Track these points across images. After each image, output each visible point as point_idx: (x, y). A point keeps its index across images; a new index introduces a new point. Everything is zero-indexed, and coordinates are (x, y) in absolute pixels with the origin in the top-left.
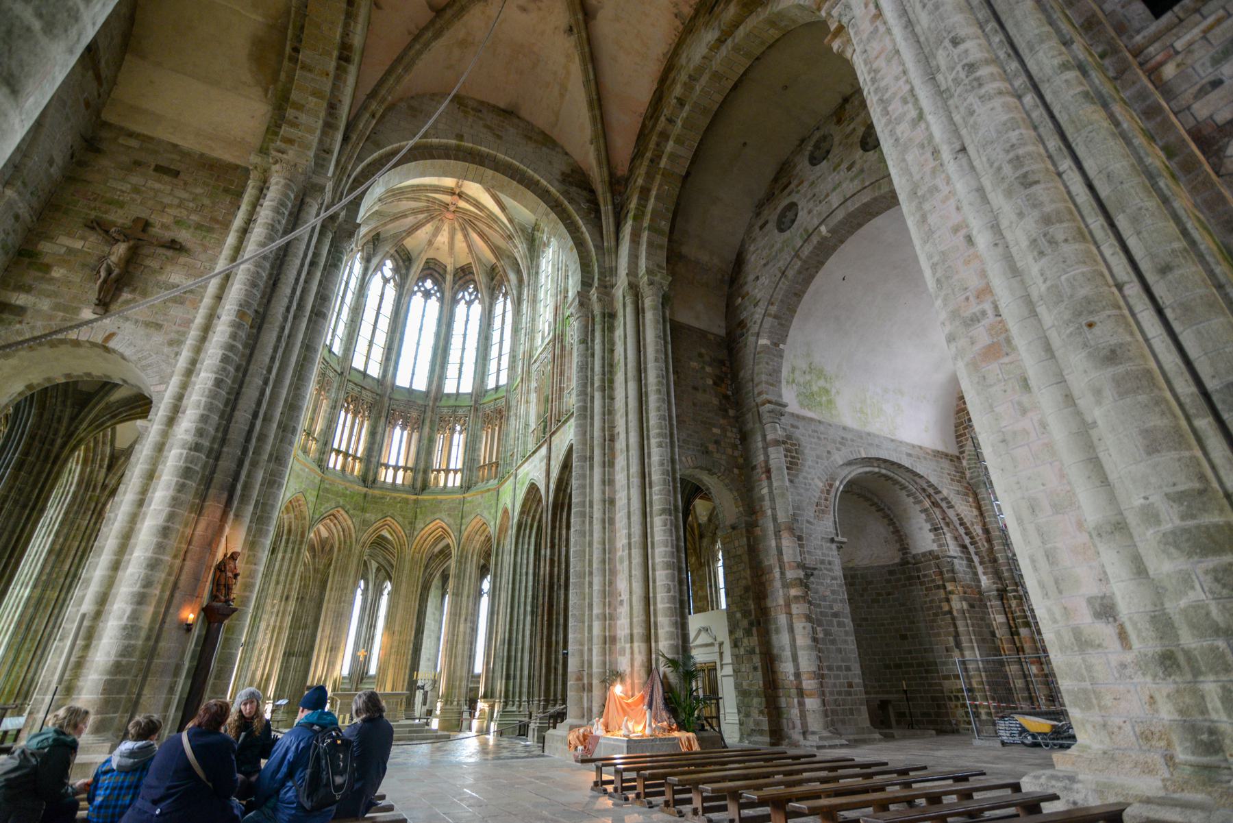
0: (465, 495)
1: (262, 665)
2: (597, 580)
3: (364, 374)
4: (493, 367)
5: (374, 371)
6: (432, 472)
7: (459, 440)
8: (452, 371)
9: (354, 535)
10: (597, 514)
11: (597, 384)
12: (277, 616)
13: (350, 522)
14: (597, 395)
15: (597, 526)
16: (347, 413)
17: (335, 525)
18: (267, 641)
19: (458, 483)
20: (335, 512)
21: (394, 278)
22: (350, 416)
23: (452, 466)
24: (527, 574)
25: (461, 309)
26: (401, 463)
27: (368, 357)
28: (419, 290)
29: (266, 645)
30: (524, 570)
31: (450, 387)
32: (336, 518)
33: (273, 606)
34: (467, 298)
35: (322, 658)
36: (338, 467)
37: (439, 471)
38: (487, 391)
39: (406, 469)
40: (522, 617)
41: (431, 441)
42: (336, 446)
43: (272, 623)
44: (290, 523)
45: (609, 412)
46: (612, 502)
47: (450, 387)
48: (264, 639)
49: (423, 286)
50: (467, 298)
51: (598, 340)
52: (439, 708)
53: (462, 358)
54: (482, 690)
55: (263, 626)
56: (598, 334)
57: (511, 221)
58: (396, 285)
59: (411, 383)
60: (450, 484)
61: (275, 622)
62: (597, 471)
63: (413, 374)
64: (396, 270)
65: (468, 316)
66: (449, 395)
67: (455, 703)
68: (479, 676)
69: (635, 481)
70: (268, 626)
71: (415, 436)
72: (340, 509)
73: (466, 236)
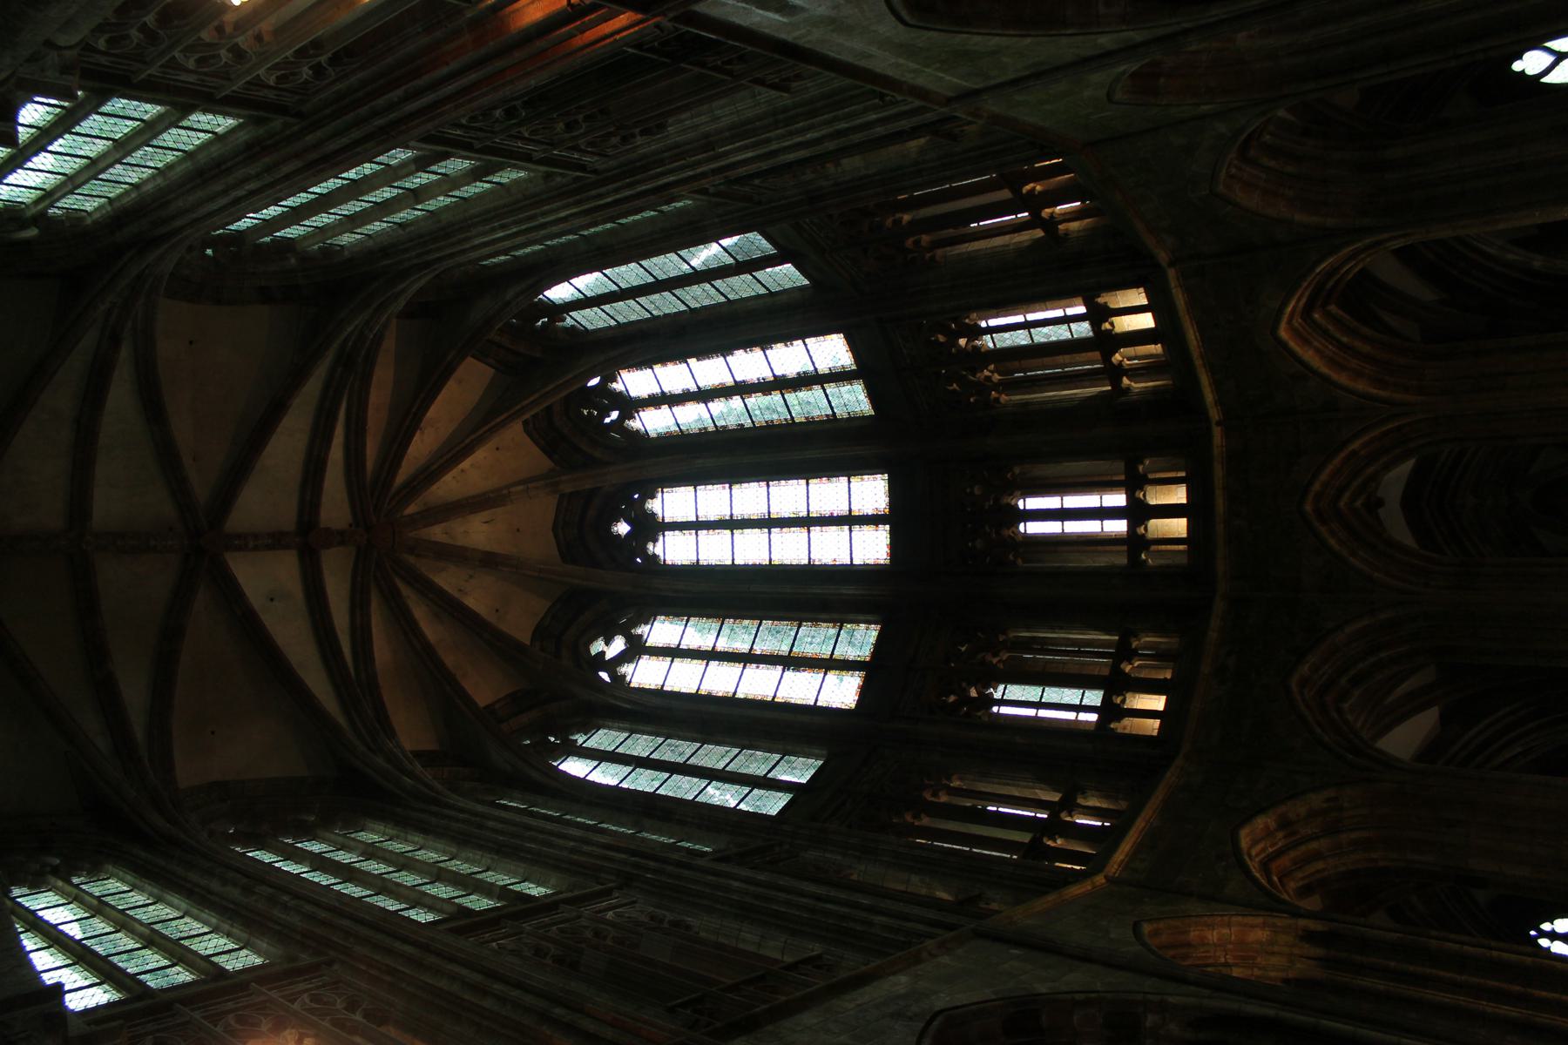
0: (1163, 257)
3: (873, 670)
4: (741, 287)
5: (860, 640)
6: (1128, 389)
8: (809, 404)
19: (1138, 298)
23: (1083, 329)
25: (654, 422)
26: (1118, 499)
31: (854, 399)
34: (615, 415)
36: (1157, 703)
37: (1115, 372)
39: (1133, 484)
41: (1028, 418)
47: (854, 399)
53: (764, 387)
57: (299, 376)
58: (648, 619)
60: (1146, 321)
73: (430, 473)
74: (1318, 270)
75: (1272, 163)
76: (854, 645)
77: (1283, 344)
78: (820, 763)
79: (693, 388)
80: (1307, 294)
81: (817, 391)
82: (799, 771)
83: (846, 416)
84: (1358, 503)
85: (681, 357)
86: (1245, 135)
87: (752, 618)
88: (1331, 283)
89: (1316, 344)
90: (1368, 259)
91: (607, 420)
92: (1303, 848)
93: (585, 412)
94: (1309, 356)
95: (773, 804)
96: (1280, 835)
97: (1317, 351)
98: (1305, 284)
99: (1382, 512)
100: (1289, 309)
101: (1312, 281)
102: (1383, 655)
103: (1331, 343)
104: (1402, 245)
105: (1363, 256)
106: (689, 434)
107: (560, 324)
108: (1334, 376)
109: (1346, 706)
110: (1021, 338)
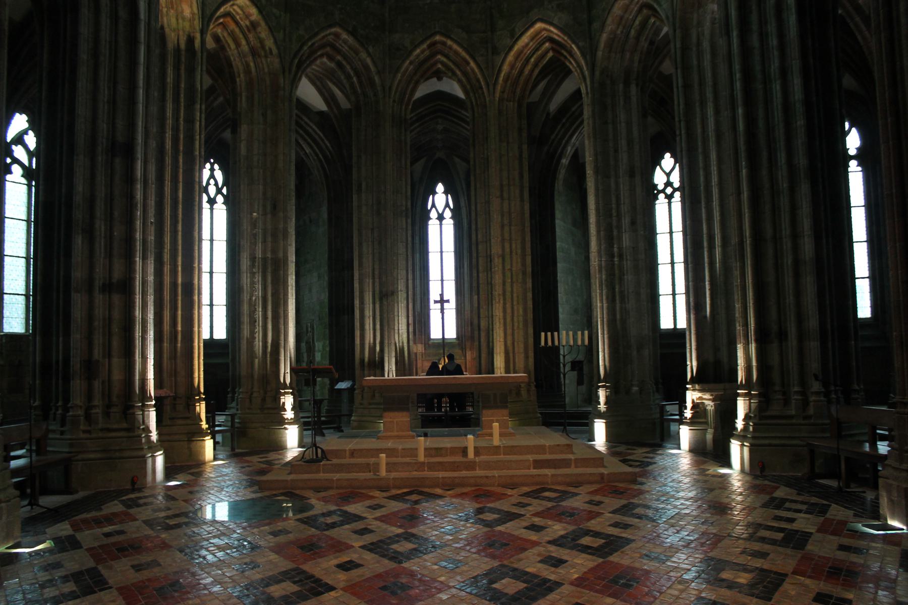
1: (259, 330)
9: (377, 79)
12: (264, 241)
13: (363, 55)
17: (339, 65)
18: (259, 287)
20: (330, 38)
24: (784, 72)
29: (260, 293)
30: (775, 66)
32: (338, 51)
33: (254, 225)
35: (368, 313)
40: (784, 185)
43: (259, 254)
44: (247, 71)
48: (253, 283)
52: (602, 399)
54: (692, 364)
55: (245, 263)
61: (264, 251)
67: (635, 389)
68: (677, 335)
70: (253, 259)
72: (337, 29)
74: (573, 46)
75: (637, 22)
77: (532, 24)
80: (560, 39)
84: (440, 66)
86: (656, 6)
88: (565, 53)
89: (531, 44)
90: (576, 73)
92: (241, 36)
94: (525, 39)
96: (248, 23)
97: (527, 45)
98: (566, 38)
99: (435, 79)
100: (552, 29)
101: (567, 43)
102: (355, 79)
103: (530, 53)
104: (582, 92)
105: (579, 71)
108: (512, 53)
109: (325, 60)
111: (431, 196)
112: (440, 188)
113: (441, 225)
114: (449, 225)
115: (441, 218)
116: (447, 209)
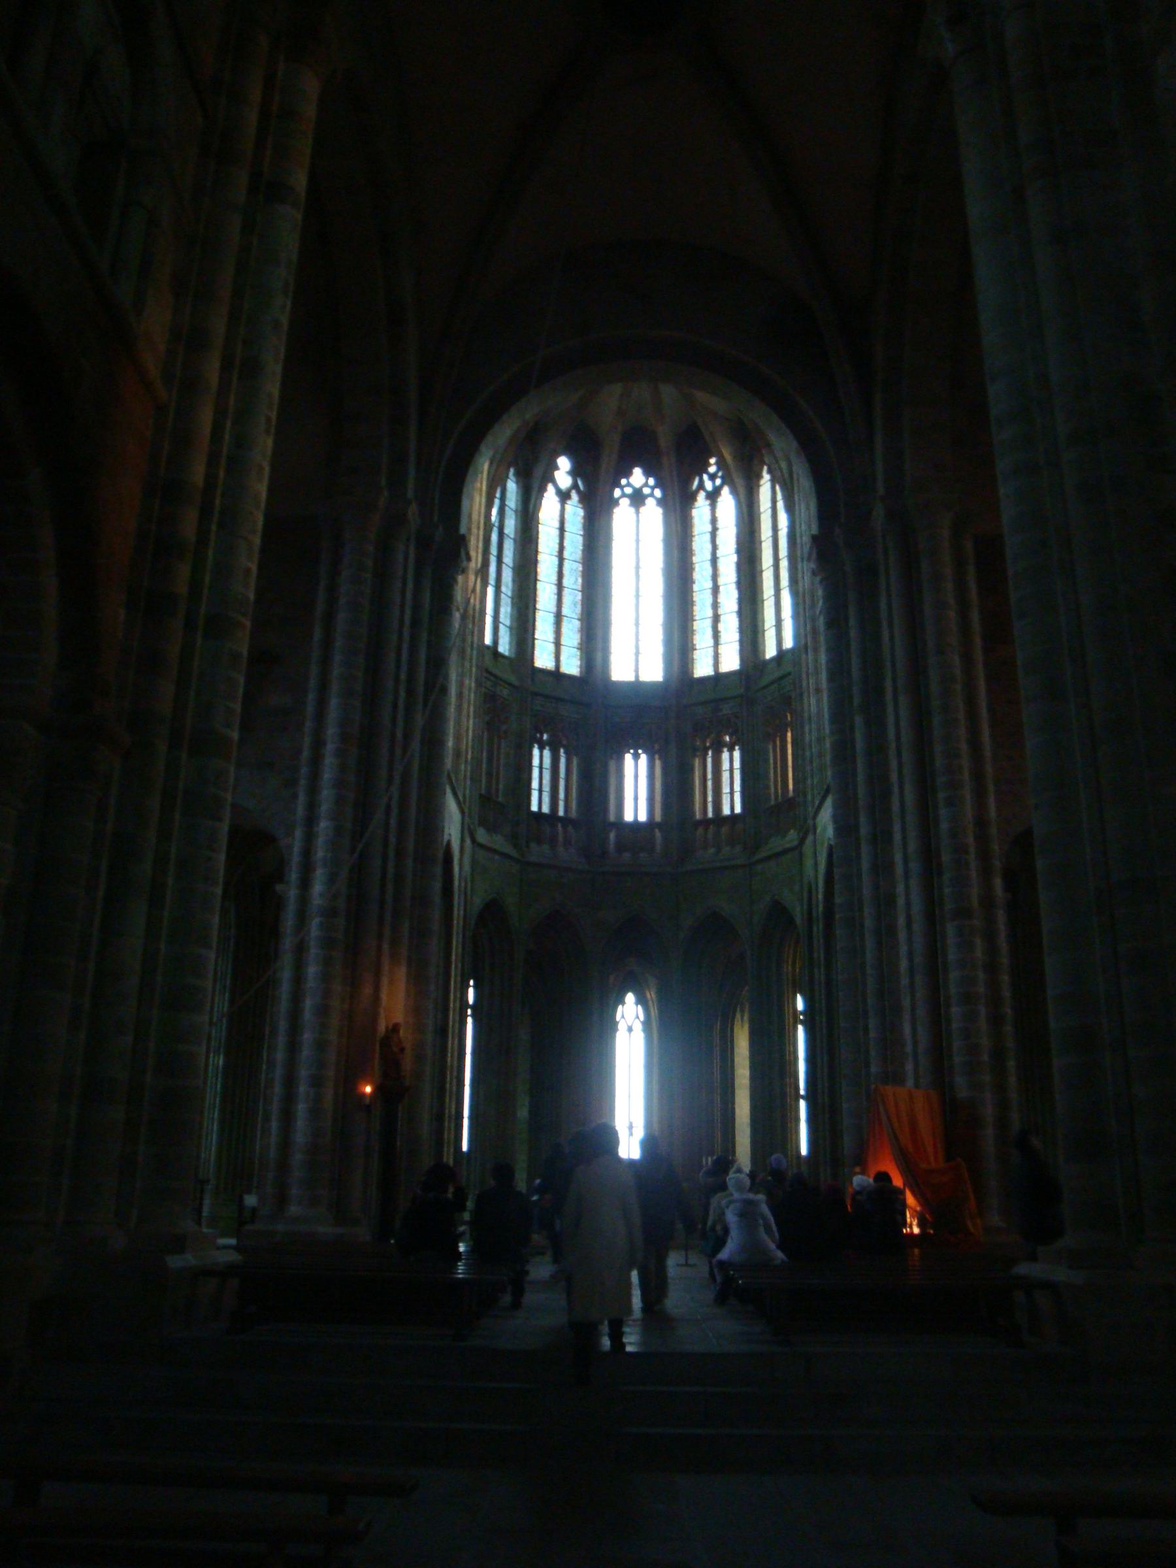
2: (872, 1023)
3: (556, 675)
5: (571, 666)
7: (732, 761)
10: (869, 923)
11: (857, 701)
14: (858, 720)
15: (870, 943)
16: (541, 749)
21: (575, 486)
22: (547, 753)
27: (558, 644)
28: (624, 495)
31: (702, 668)
38: (766, 663)
42: (534, 807)
45: (877, 747)
46: (891, 900)
49: (629, 485)
50: (709, 485)
51: (852, 622)
53: (715, 605)
56: (852, 611)
59: (637, 671)
62: (865, 850)
63: (637, 653)
64: (574, 473)
65: (714, 521)
66: (703, 680)
69: (915, 866)
71: (658, 763)
76: (568, 659)
78: (507, 653)
79: (719, 553)
81: (711, 642)
82: (504, 647)
83: (695, 657)
85: (739, 551)
87: (583, 585)
91: (705, 477)
93: (713, 461)
95: (488, 640)
106: (691, 541)
107: (765, 468)
110: (726, 765)
111: (620, 1007)
112: (630, 998)
113: (630, 1037)
114: (639, 1036)
115: (630, 1029)
116: (637, 1020)
